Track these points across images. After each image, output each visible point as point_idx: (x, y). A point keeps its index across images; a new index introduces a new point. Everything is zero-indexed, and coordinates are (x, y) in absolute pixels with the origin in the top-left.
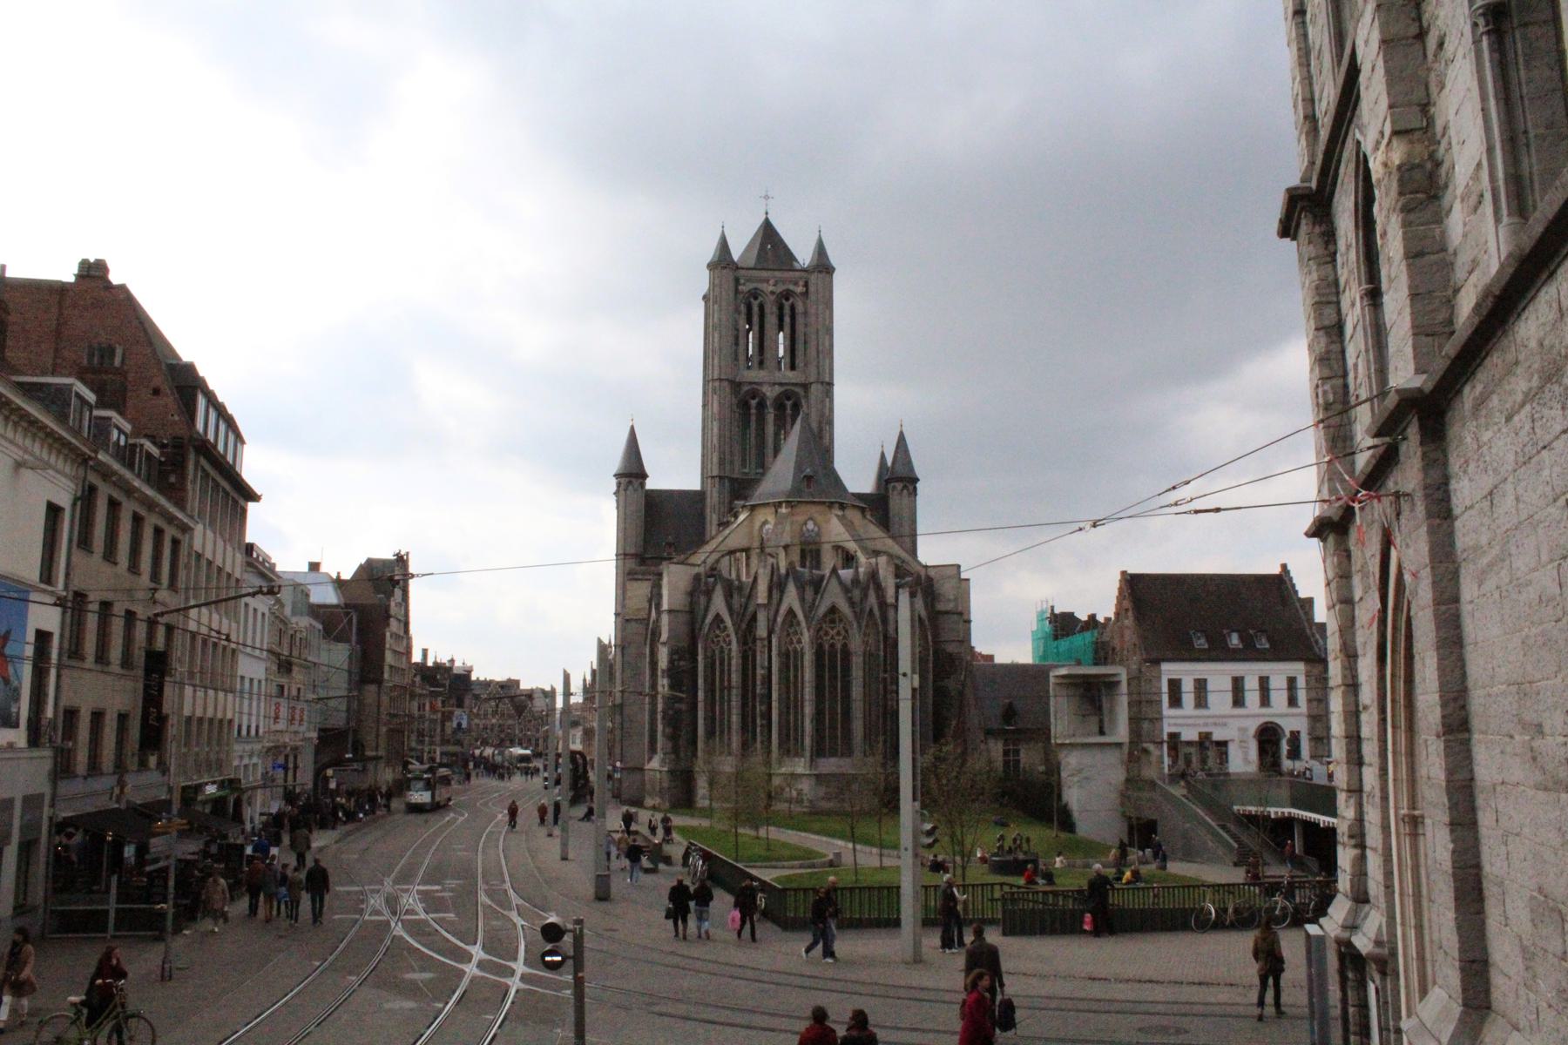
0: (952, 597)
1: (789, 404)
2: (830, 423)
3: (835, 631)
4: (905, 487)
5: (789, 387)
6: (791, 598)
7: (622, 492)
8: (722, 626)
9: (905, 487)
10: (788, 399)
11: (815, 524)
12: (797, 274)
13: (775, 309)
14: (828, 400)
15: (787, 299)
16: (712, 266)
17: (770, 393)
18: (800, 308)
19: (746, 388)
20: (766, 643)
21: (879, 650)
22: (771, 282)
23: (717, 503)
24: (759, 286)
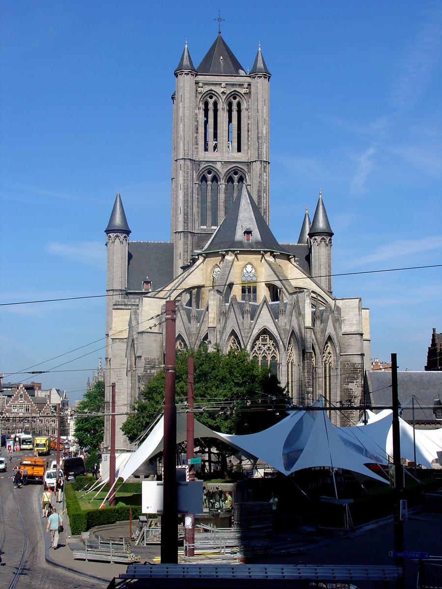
0: (355, 322)
1: (236, 177)
3: (266, 347)
5: (236, 165)
10: (236, 173)
13: (226, 107)
15: (235, 98)
17: (222, 170)
18: (244, 106)
19: (203, 166)
22: (223, 85)
23: (182, 253)
24: (213, 88)
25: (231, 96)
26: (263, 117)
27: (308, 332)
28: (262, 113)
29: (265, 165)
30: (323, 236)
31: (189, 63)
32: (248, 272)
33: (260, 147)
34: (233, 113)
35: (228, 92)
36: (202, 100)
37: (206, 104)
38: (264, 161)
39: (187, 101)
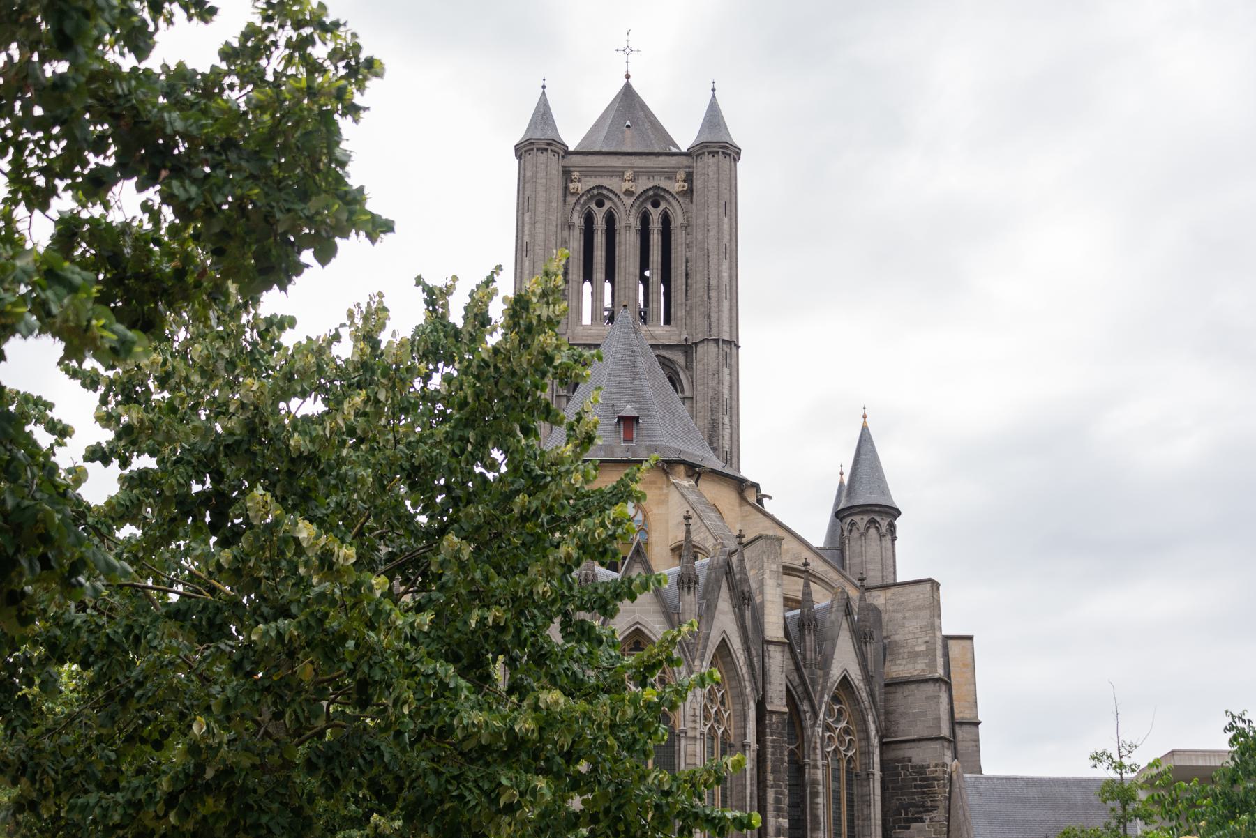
0: (923, 648)
2: (732, 409)
4: (873, 521)
9: (873, 521)
12: (673, 161)
13: (634, 221)
14: (726, 371)
15: (656, 205)
16: (523, 150)
18: (677, 220)
22: (628, 174)
24: (605, 182)
25: (645, 201)
26: (719, 240)
27: (772, 654)
28: (719, 231)
29: (726, 348)
30: (873, 516)
33: (714, 309)
34: (651, 236)
36: (578, 208)
37: (589, 219)
38: (723, 340)
39: (541, 208)
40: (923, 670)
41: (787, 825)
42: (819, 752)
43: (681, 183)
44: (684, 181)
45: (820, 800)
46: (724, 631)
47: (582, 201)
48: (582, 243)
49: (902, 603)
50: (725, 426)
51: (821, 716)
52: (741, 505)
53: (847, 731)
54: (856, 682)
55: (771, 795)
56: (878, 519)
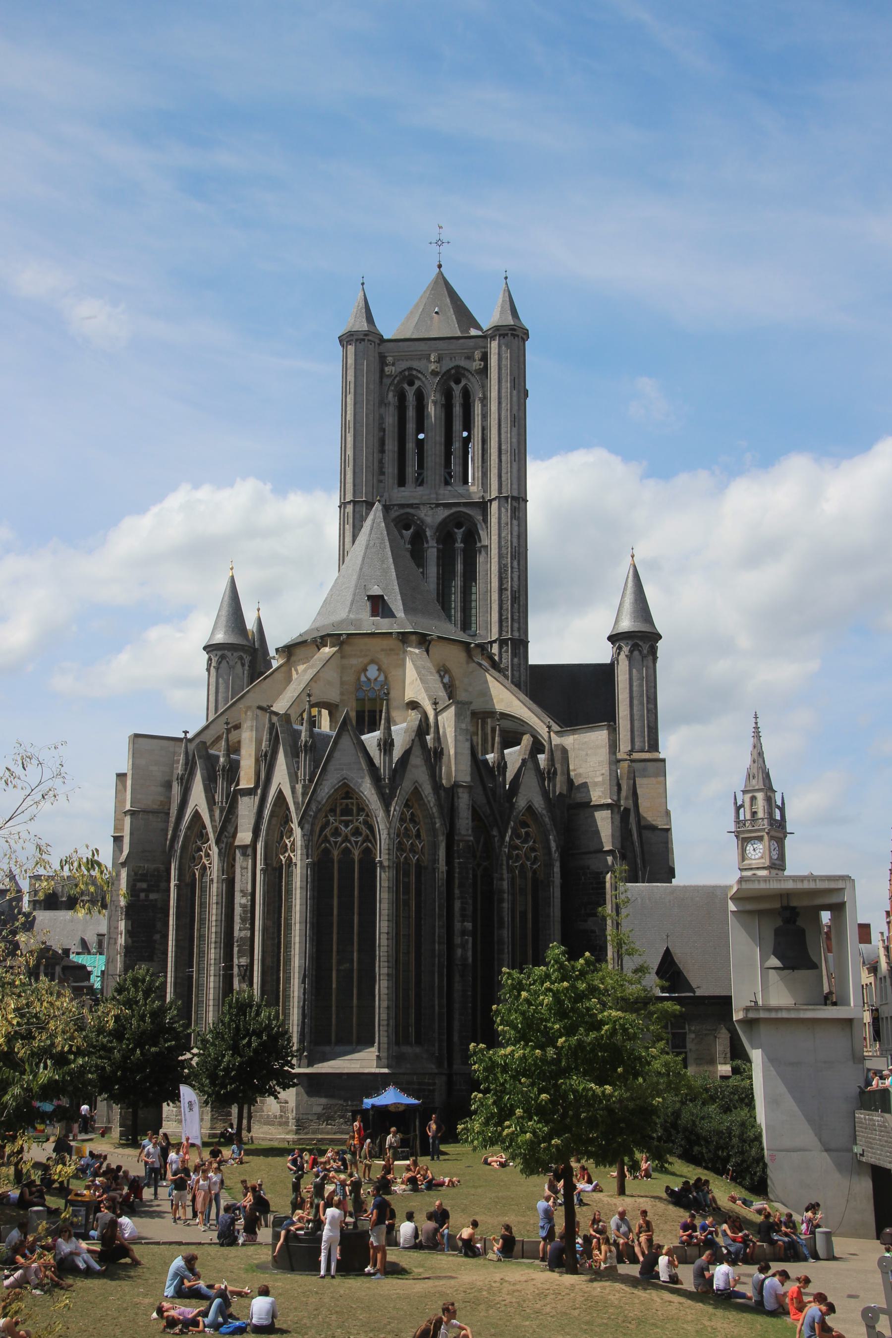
1: (459, 533)
6: (281, 777)
7: (213, 670)
8: (204, 831)
10: (459, 526)
11: (379, 670)
12: (471, 343)
15: (458, 382)
20: (249, 851)
21: (435, 861)
24: (415, 364)
27: (460, 795)
31: (364, 320)
32: (369, 679)
34: (454, 409)
35: (444, 369)
37: (402, 397)
40: (600, 797)
41: (470, 928)
42: (505, 867)
43: (478, 362)
44: (481, 360)
45: (505, 905)
46: (416, 782)
47: (396, 382)
48: (396, 418)
49: (586, 742)
50: (514, 570)
51: (507, 839)
52: (468, 663)
53: (533, 849)
54: (540, 810)
55: (457, 905)
56: (640, 643)
